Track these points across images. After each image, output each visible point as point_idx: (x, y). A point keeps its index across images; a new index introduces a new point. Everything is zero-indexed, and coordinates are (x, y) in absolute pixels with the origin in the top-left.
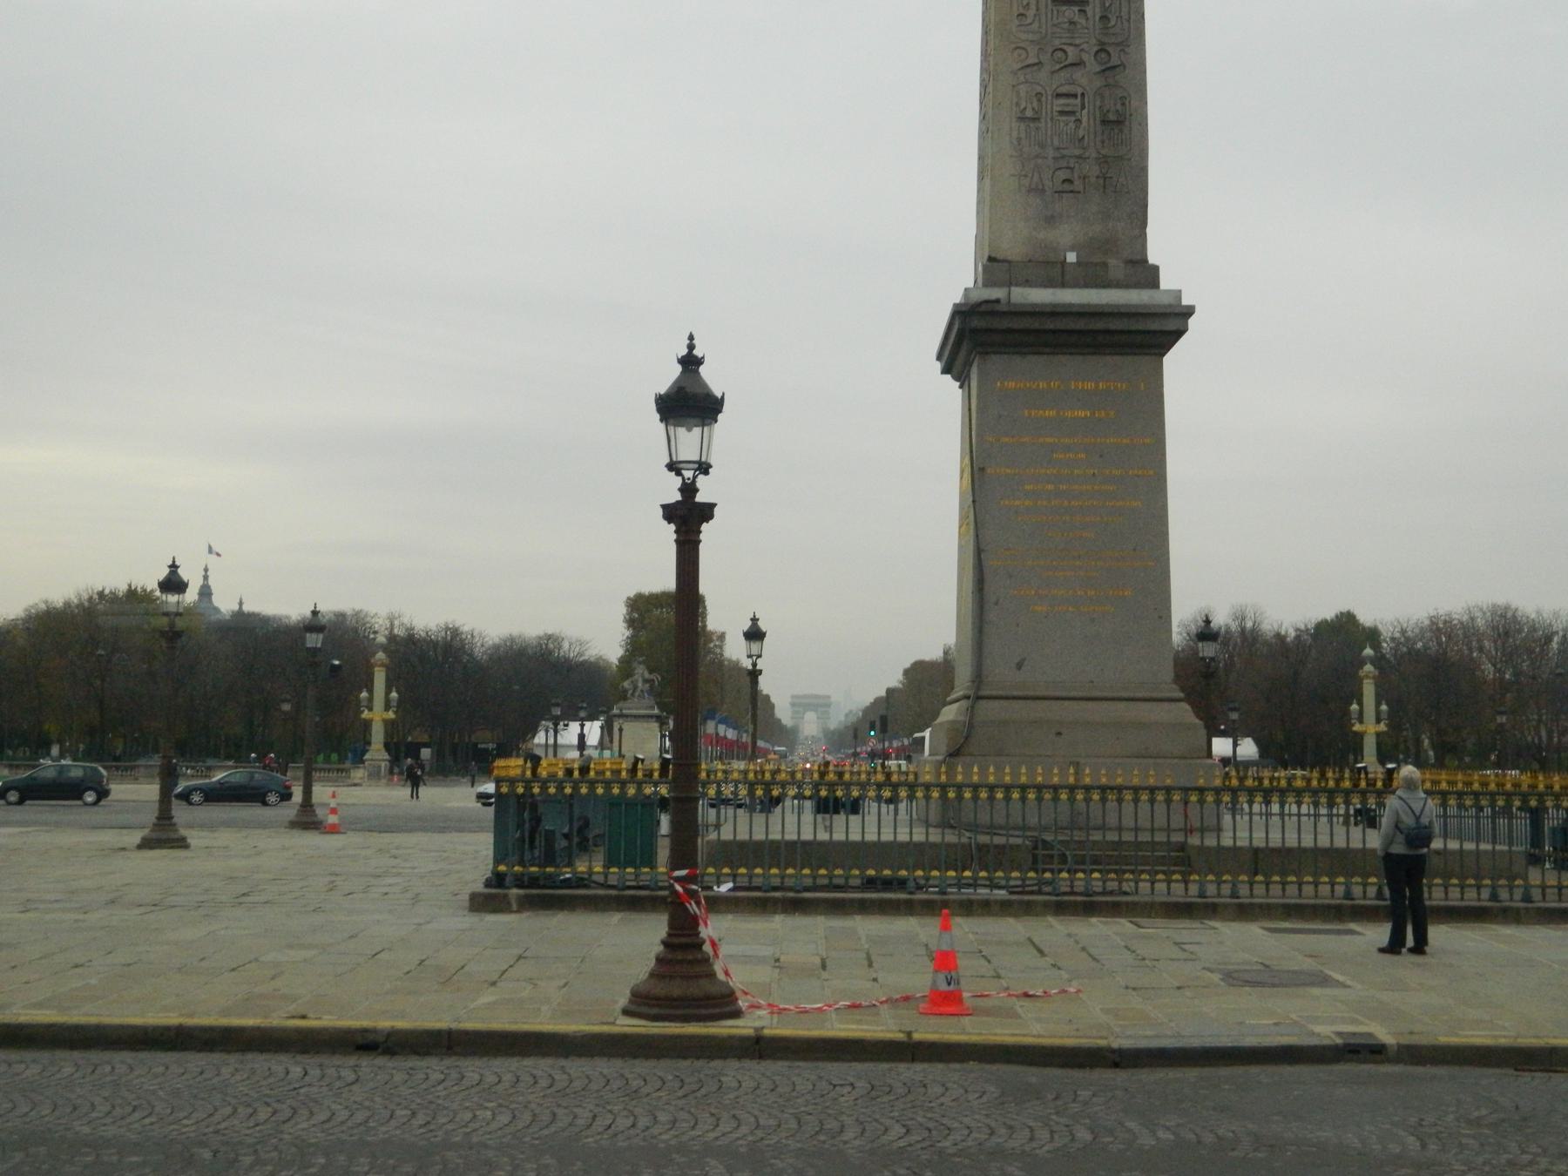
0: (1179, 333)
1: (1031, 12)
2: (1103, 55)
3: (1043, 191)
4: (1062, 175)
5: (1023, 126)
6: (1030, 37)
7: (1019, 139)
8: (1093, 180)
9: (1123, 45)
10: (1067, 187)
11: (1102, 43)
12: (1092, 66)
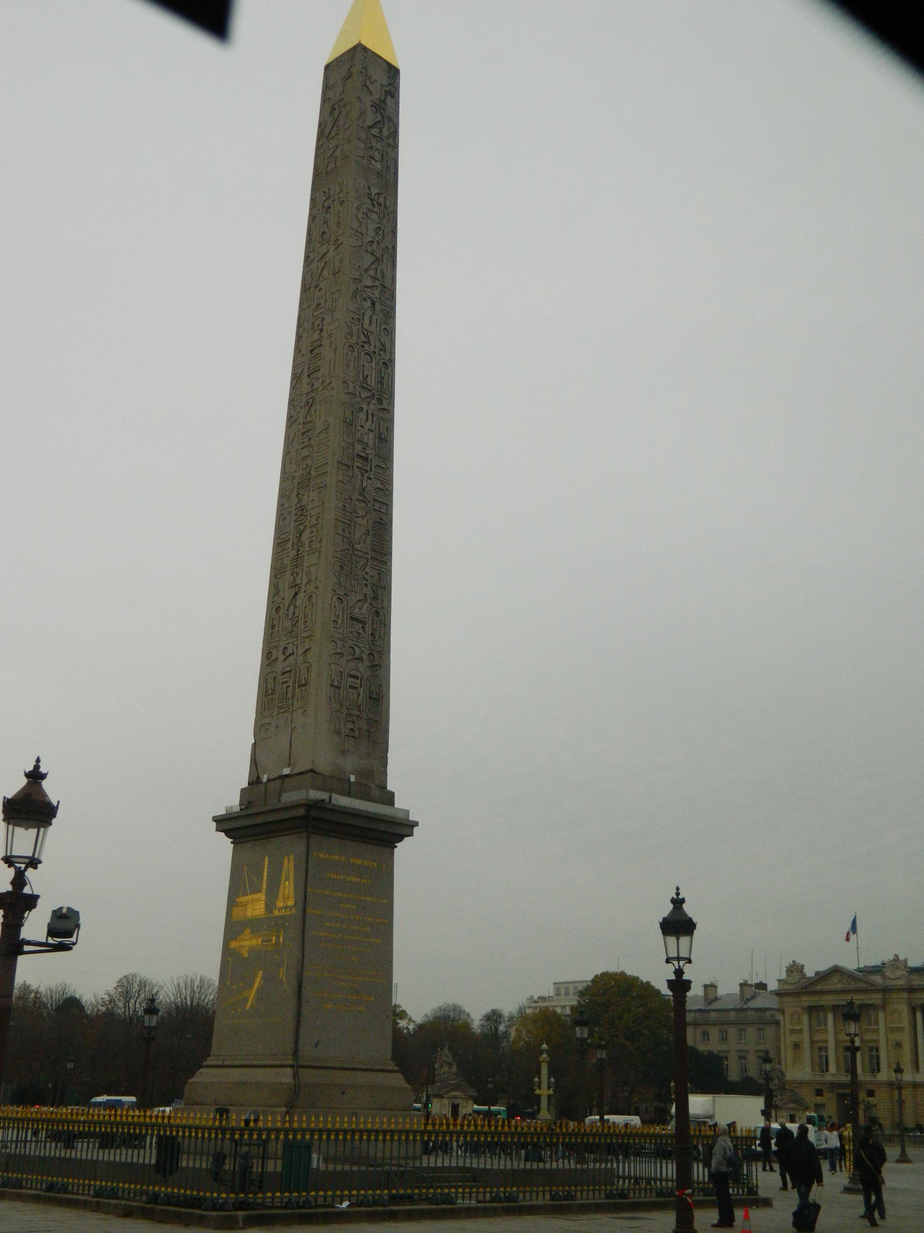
4: (350, 725)
8: (364, 732)
10: (351, 734)
12: (367, 663)
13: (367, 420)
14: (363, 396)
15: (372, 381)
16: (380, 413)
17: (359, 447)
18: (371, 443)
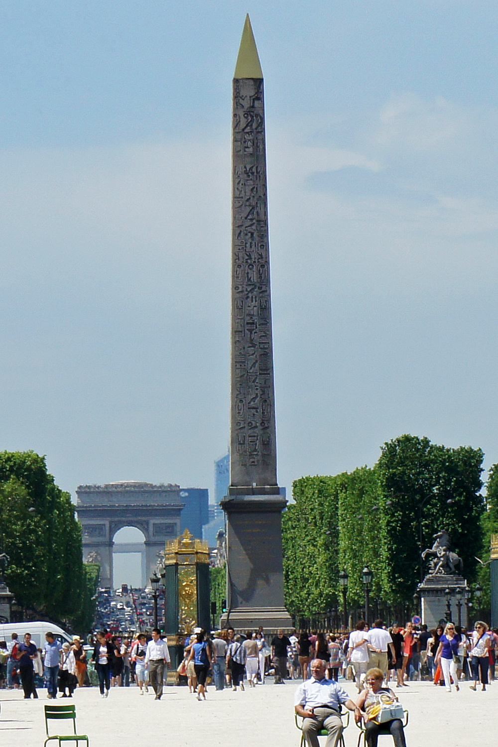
2: (263, 424)
3: (246, 465)
4: (252, 460)
5: (240, 446)
6: (241, 419)
7: (239, 450)
9: (268, 421)
10: (253, 463)
11: (263, 420)
13: (252, 302)
14: (249, 290)
15: (254, 277)
16: (261, 295)
17: (247, 319)
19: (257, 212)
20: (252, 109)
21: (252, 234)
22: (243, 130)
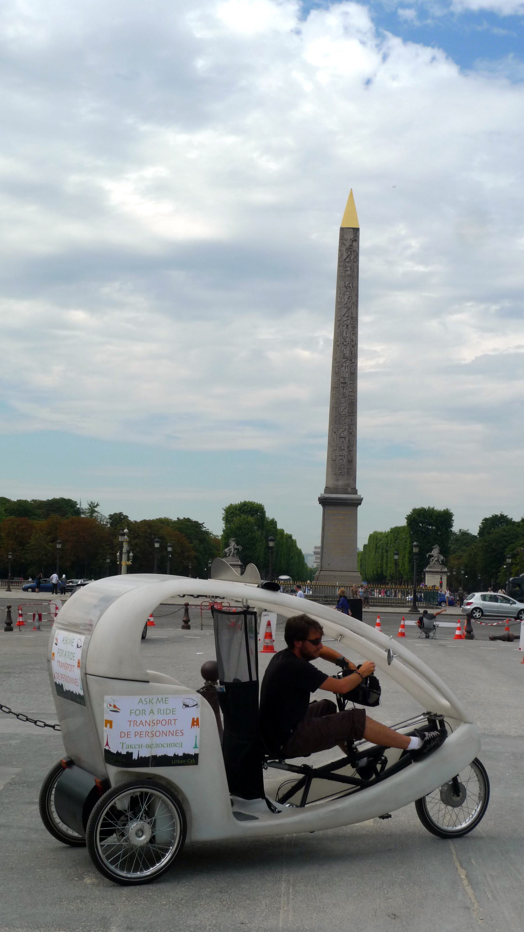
0: (360, 504)
1: (335, 439)
9: (352, 446)
12: (346, 450)
15: (348, 354)
18: (347, 377)
19: (352, 312)
20: (351, 247)
21: (347, 326)
22: (345, 260)
